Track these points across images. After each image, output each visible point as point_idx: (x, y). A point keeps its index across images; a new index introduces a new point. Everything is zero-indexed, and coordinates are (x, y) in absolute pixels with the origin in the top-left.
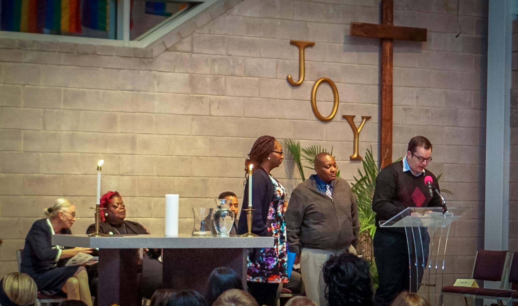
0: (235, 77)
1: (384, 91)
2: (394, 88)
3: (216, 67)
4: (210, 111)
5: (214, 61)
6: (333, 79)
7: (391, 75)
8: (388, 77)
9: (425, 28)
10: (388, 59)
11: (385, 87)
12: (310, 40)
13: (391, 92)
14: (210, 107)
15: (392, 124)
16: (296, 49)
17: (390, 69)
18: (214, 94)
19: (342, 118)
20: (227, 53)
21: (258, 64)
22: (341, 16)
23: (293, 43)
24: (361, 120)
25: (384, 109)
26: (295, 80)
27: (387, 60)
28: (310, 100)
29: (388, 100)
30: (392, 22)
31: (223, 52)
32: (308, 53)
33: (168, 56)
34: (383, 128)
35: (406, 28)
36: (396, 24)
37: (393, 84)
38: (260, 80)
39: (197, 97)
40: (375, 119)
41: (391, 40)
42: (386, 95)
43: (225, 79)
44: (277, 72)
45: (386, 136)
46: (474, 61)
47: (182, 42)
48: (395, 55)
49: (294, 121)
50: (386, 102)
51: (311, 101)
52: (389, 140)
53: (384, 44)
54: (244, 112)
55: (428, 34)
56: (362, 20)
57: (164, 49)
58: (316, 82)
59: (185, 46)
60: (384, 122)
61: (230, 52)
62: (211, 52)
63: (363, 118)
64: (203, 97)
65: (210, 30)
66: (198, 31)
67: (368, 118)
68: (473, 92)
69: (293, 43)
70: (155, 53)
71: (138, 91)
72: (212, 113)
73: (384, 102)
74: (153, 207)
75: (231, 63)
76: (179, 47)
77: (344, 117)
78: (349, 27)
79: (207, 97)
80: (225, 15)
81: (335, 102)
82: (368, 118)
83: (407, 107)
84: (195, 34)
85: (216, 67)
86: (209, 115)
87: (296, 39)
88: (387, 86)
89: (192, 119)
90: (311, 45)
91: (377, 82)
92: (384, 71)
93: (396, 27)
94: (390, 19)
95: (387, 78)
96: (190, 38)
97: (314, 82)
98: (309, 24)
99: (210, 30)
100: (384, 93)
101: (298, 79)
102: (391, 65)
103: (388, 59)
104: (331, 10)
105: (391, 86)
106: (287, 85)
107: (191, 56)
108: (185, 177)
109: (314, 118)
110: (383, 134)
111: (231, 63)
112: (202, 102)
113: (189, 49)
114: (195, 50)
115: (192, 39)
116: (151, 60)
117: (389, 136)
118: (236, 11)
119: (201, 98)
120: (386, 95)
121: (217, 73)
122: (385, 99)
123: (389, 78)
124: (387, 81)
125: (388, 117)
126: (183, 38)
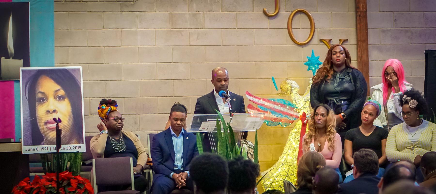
0: (213, 12)
1: (358, 16)
2: (368, 14)
4: (190, 41)
6: (307, 10)
11: (359, 14)
13: (366, 17)
14: (189, 38)
18: (193, 28)
19: (319, 41)
26: (271, 12)
29: (362, 24)
37: (367, 11)
39: (177, 31)
42: (360, 20)
43: (204, 15)
44: (253, 6)
49: (271, 46)
50: (360, 27)
51: (288, 29)
52: (364, 57)
54: (222, 42)
58: (292, 12)
64: (182, 31)
72: (192, 43)
74: (139, 123)
77: (321, 41)
79: (187, 30)
81: (311, 28)
88: (361, 12)
91: (353, 9)
95: (361, 5)
97: (291, 12)
101: (274, 11)
105: (366, 12)
108: (168, 97)
109: (292, 43)
119: (180, 32)
120: (360, 20)
121: (195, 10)
123: (363, 6)
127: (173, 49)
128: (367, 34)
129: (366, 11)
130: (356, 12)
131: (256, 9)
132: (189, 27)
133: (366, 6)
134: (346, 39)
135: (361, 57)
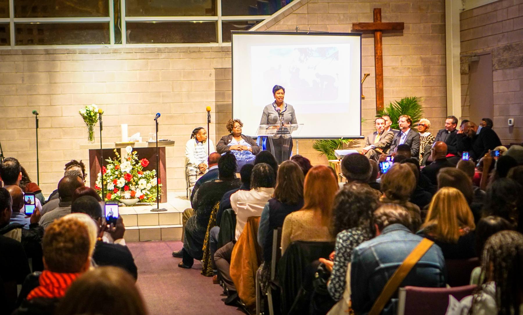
2: (383, 57)
7: (381, 50)
8: (379, 51)
9: (403, 22)
10: (379, 41)
11: (377, 57)
13: (381, 59)
15: (382, 77)
17: (380, 46)
22: (349, 20)
24: (364, 76)
25: (377, 68)
27: (378, 42)
29: (379, 64)
30: (381, 20)
34: (377, 80)
35: (389, 23)
36: (383, 21)
37: (383, 55)
40: (373, 74)
41: (380, 31)
42: (378, 61)
45: (379, 84)
46: (440, 38)
48: (383, 38)
52: (381, 86)
53: (376, 33)
55: (405, 25)
56: (363, 20)
60: (377, 77)
63: (365, 75)
67: (368, 75)
68: (440, 56)
73: (377, 65)
78: (351, 25)
80: (275, 25)
82: (368, 75)
83: (395, 67)
91: (374, 54)
92: (376, 48)
93: (383, 23)
94: (379, 19)
95: (379, 52)
98: (328, 26)
100: (376, 60)
102: (381, 44)
103: (379, 41)
104: (342, 17)
105: (382, 56)
110: (377, 83)
117: (381, 84)
118: (281, 23)
120: (378, 61)
122: (378, 63)
124: (379, 54)
125: (379, 74)
128: (382, 70)
129: (381, 54)
130: (375, 56)
133: (382, 52)
134: (368, 73)
135: (379, 85)
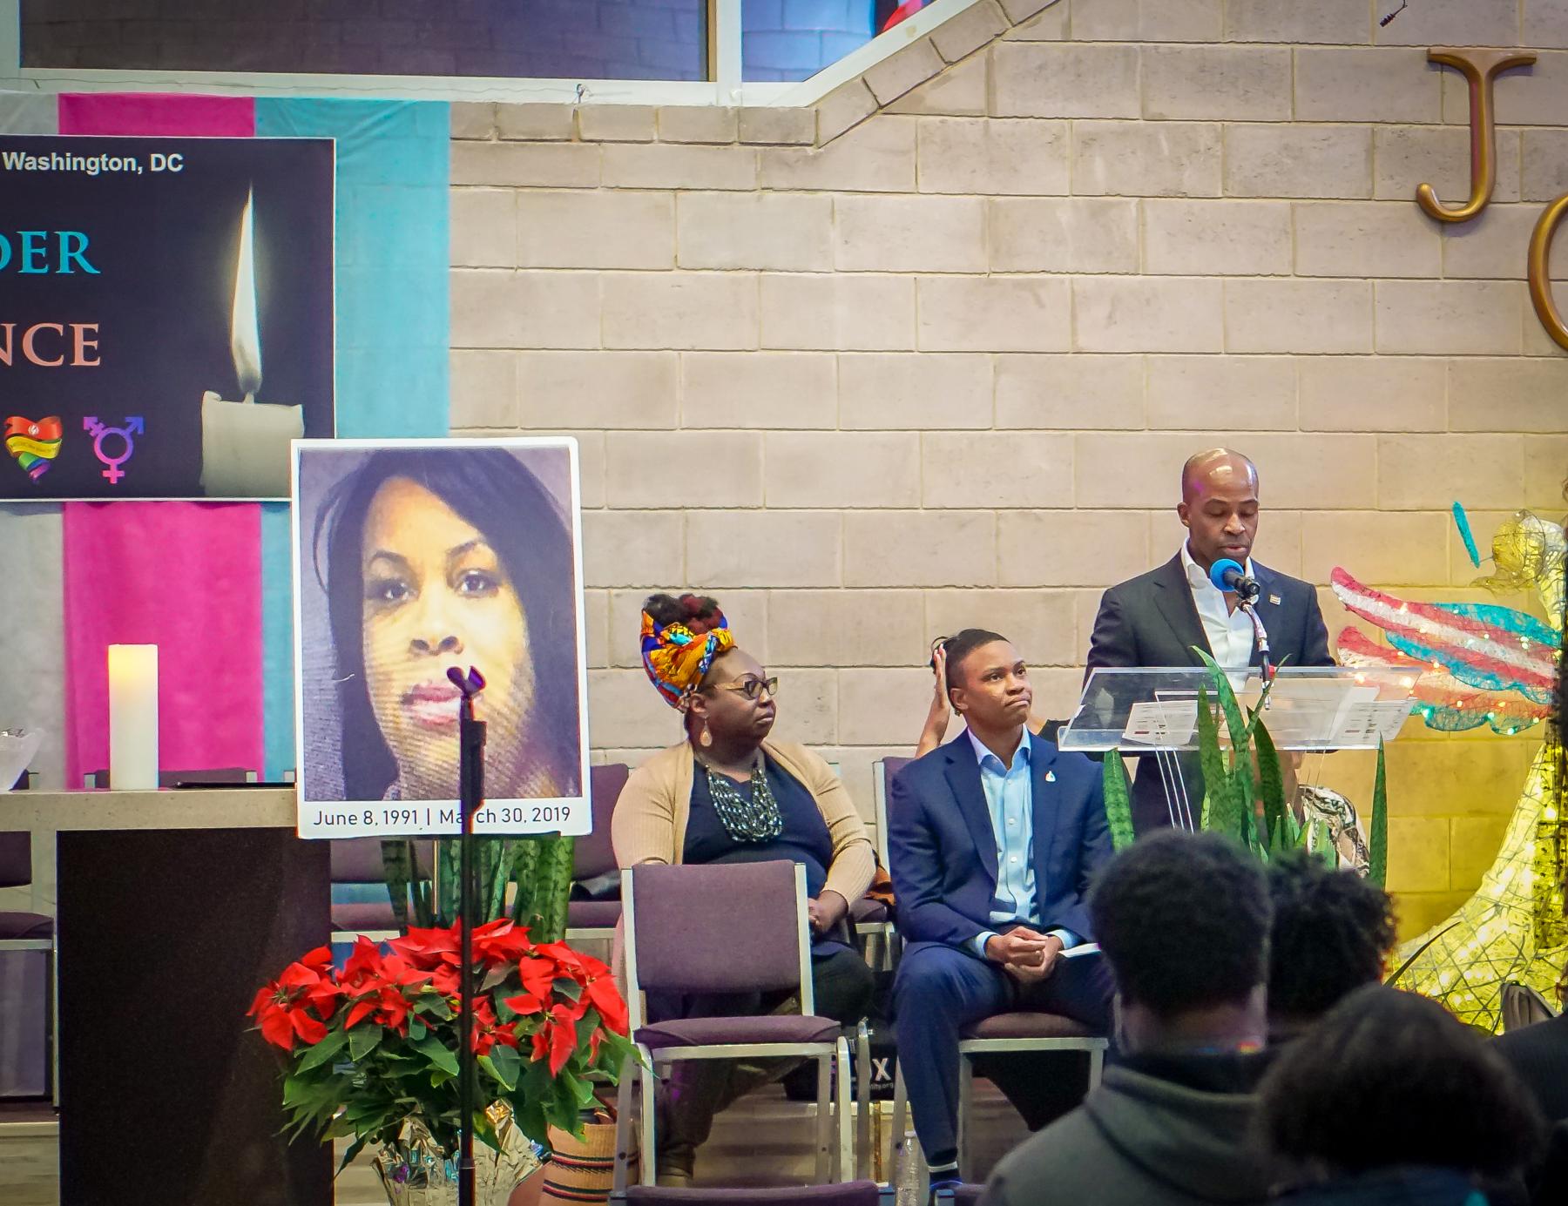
3: (1099, 165)
4: (1074, 332)
5: (1088, 142)
12: (1521, 46)
14: (1074, 317)
16: (1456, 85)
20: (1143, 109)
21: (1286, 147)
23: (1439, 62)
26: (1453, 200)
28: (1526, 277)
31: (1132, 108)
32: (1509, 97)
33: (885, 127)
38: (1293, 208)
39: (1018, 285)
43: (1141, 210)
44: (1371, 174)
47: (948, 78)
51: (1532, 280)
57: (870, 105)
58: (1551, 203)
59: (962, 89)
61: (1154, 109)
62: (1074, 109)
64: (1042, 283)
65: (1067, 27)
66: (1012, 33)
69: (1439, 62)
70: (831, 126)
71: (761, 270)
75: (1164, 144)
76: (935, 96)
79: (1062, 282)
84: (999, 44)
85: (1099, 165)
86: (1069, 348)
87: (1451, 43)
89: (996, 370)
90: (1521, 65)
96: (982, 55)
99: (1067, 27)
101: (1466, 196)
106: (1418, 221)
107: (987, 125)
111: (1164, 144)
112: (1040, 304)
113: (977, 102)
114: (1004, 104)
115: (989, 63)
116: (810, 151)
126: (950, 63)
127: (995, 367)
131: (1382, 187)
132: (1071, 266)
